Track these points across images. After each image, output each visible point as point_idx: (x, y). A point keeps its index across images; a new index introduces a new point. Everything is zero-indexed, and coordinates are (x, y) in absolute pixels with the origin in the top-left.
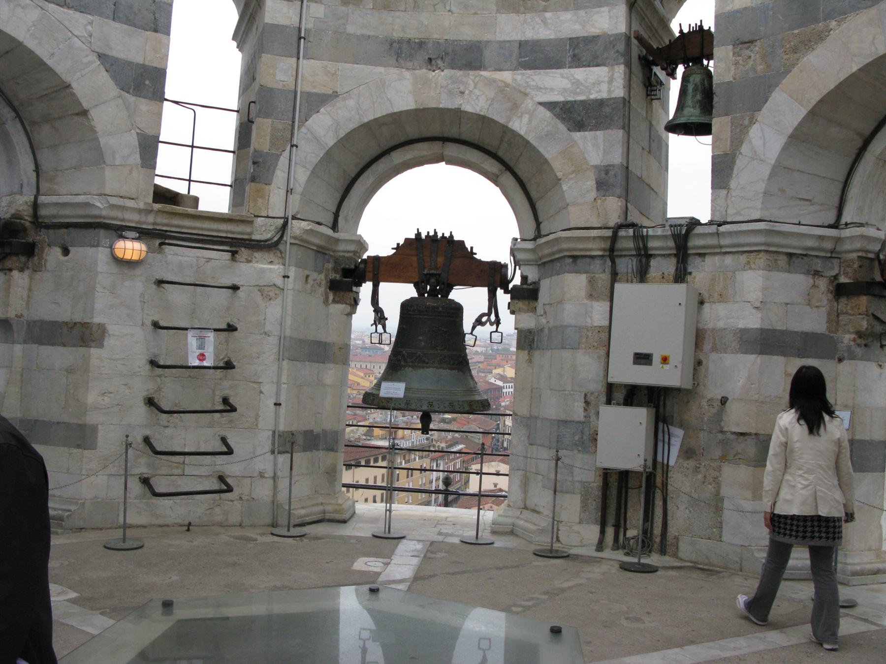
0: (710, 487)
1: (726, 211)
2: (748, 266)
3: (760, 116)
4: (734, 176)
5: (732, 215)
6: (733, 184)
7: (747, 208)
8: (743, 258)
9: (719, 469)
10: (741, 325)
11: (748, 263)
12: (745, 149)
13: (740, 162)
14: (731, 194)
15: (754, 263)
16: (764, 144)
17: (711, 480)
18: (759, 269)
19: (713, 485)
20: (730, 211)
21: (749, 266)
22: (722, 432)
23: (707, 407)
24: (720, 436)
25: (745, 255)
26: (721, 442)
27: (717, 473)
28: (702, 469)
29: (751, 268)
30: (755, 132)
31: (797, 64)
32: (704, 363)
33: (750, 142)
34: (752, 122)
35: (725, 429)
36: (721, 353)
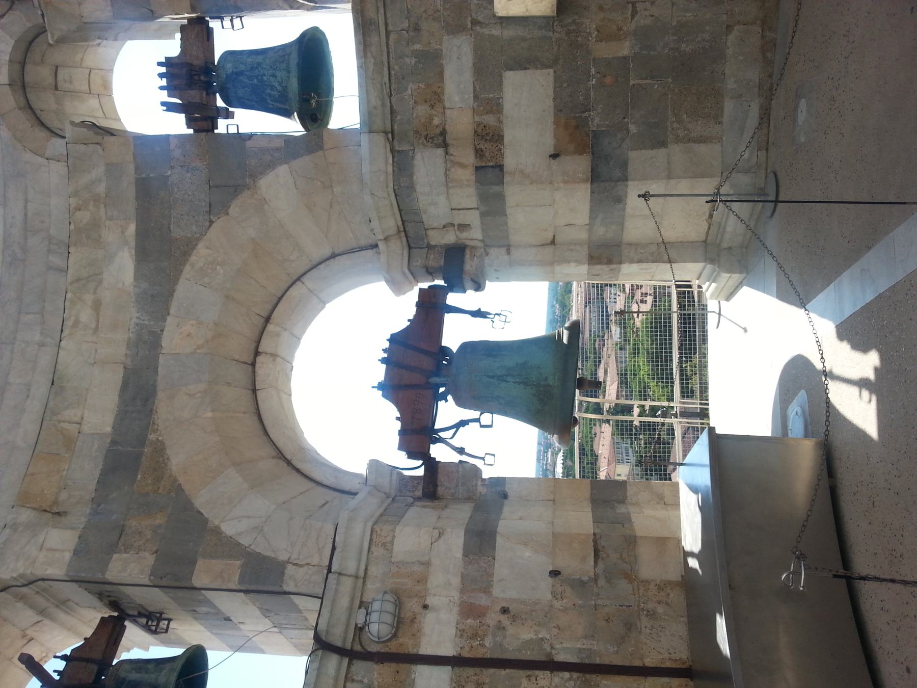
0: (672, 595)
1: (314, 566)
2: (388, 546)
3: (214, 521)
4: (273, 556)
5: (321, 559)
6: (283, 557)
7: (318, 539)
8: (378, 552)
9: (646, 582)
10: (459, 554)
11: (384, 545)
12: (245, 541)
13: (261, 548)
14: (296, 559)
15: (385, 537)
16: (249, 517)
17: (662, 594)
18: (394, 531)
19: (669, 591)
20: (315, 560)
21: (388, 544)
22: (596, 579)
23: (564, 601)
24: (602, 582)
25: (373, 548)
26: (609, 580)
27: (652, 586)
28: (650, 606)
29: (392, 543)
30: (229, 529)
31: (175, 477)
32: (505, 605)
33: (240, 534)
34: (217, 531)
35: (592, 574)
36: (492, 581)
